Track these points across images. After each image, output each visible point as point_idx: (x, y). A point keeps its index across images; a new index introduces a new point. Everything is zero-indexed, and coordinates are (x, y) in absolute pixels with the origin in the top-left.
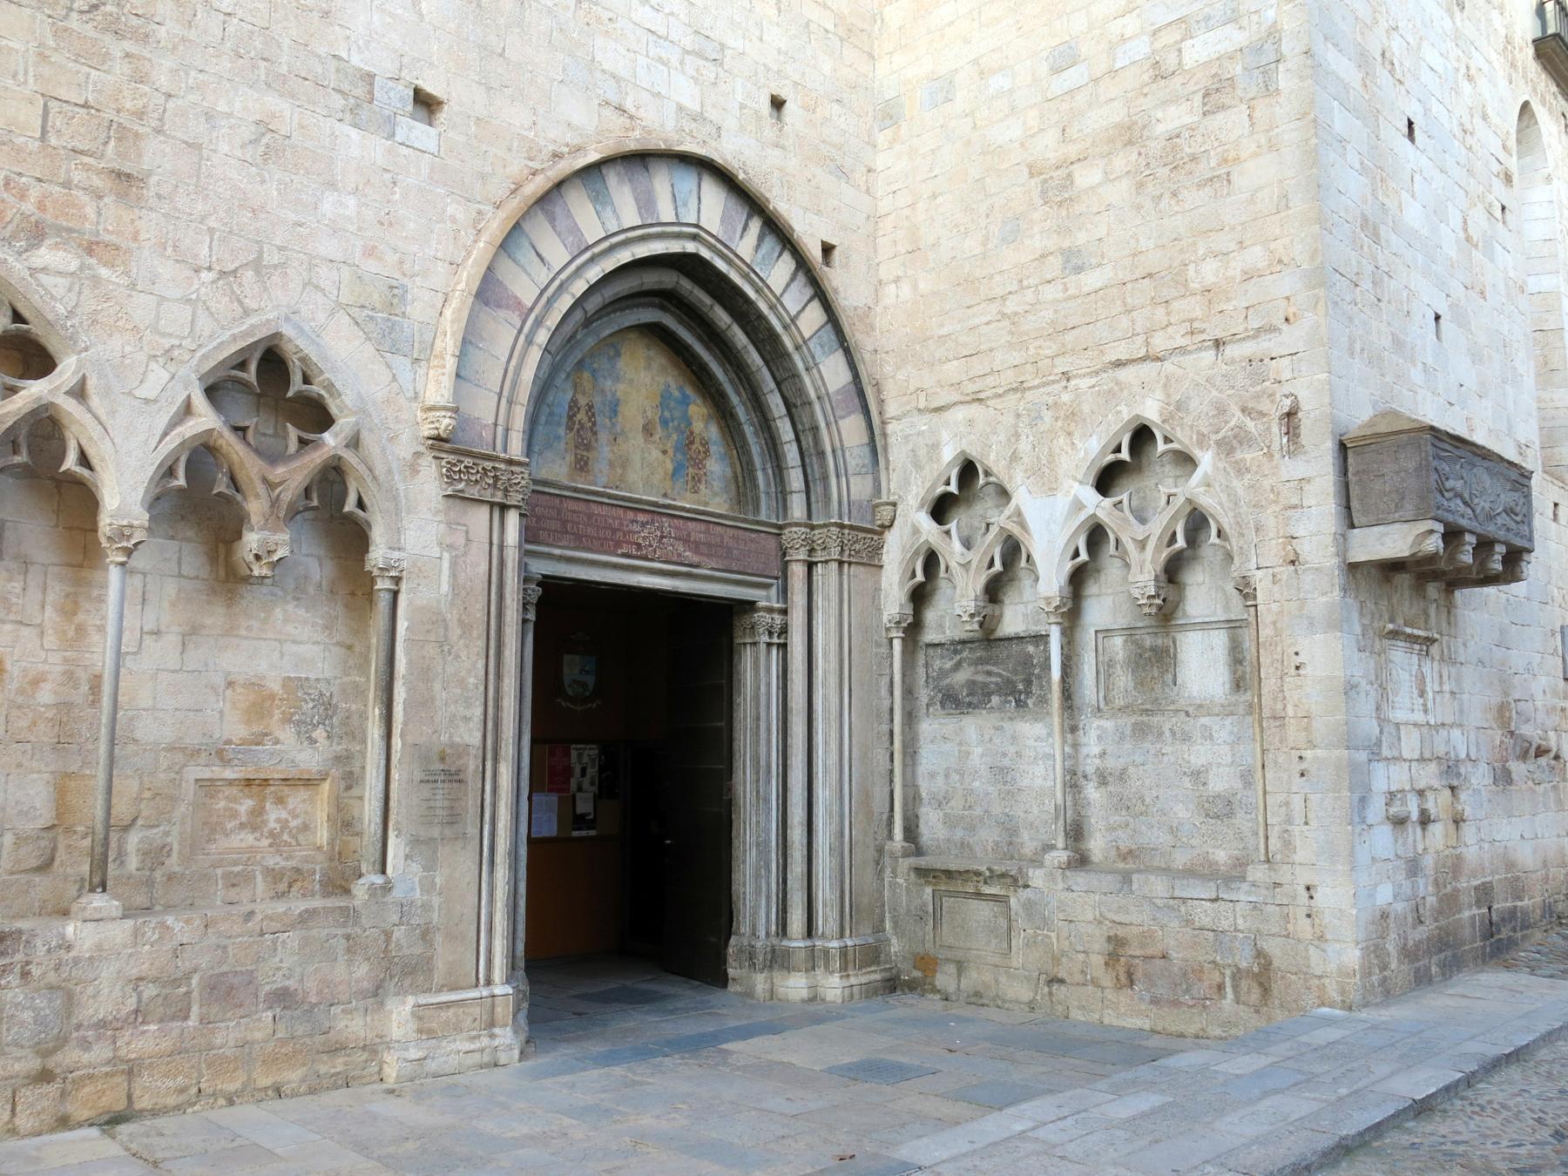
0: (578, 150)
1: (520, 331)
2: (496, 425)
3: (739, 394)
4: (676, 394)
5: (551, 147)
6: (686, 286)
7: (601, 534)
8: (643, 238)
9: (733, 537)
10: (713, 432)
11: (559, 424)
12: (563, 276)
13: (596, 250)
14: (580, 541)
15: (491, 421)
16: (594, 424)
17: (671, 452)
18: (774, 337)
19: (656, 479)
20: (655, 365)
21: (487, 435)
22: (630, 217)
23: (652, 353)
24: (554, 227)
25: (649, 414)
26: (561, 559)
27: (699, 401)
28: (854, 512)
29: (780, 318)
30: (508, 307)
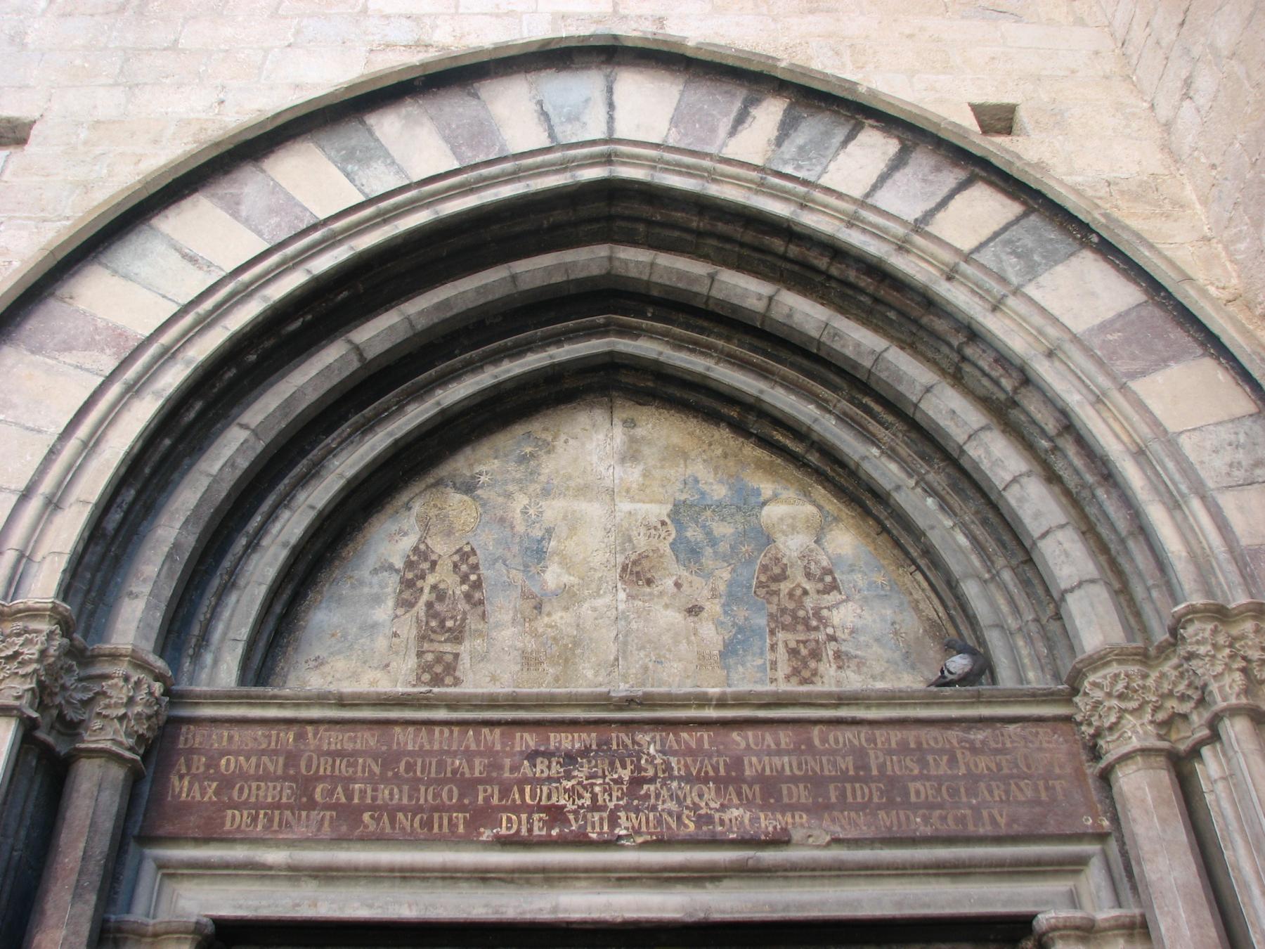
3: (872, 440)
4: (719, 492)
6: (634, 260)
7: (426, 796)
9: (904, 748)
10: (845, 541)
11: (377, 600)
14: (349, 822)
16: (477, 585)
17: (713, 608)
18: (877, 270)
20: (650, 454)
23: (639, 432)
24: (235, 215)
26: (295, 873)
27: (791, 493)
29: (879, 234)
30: (88, 346)
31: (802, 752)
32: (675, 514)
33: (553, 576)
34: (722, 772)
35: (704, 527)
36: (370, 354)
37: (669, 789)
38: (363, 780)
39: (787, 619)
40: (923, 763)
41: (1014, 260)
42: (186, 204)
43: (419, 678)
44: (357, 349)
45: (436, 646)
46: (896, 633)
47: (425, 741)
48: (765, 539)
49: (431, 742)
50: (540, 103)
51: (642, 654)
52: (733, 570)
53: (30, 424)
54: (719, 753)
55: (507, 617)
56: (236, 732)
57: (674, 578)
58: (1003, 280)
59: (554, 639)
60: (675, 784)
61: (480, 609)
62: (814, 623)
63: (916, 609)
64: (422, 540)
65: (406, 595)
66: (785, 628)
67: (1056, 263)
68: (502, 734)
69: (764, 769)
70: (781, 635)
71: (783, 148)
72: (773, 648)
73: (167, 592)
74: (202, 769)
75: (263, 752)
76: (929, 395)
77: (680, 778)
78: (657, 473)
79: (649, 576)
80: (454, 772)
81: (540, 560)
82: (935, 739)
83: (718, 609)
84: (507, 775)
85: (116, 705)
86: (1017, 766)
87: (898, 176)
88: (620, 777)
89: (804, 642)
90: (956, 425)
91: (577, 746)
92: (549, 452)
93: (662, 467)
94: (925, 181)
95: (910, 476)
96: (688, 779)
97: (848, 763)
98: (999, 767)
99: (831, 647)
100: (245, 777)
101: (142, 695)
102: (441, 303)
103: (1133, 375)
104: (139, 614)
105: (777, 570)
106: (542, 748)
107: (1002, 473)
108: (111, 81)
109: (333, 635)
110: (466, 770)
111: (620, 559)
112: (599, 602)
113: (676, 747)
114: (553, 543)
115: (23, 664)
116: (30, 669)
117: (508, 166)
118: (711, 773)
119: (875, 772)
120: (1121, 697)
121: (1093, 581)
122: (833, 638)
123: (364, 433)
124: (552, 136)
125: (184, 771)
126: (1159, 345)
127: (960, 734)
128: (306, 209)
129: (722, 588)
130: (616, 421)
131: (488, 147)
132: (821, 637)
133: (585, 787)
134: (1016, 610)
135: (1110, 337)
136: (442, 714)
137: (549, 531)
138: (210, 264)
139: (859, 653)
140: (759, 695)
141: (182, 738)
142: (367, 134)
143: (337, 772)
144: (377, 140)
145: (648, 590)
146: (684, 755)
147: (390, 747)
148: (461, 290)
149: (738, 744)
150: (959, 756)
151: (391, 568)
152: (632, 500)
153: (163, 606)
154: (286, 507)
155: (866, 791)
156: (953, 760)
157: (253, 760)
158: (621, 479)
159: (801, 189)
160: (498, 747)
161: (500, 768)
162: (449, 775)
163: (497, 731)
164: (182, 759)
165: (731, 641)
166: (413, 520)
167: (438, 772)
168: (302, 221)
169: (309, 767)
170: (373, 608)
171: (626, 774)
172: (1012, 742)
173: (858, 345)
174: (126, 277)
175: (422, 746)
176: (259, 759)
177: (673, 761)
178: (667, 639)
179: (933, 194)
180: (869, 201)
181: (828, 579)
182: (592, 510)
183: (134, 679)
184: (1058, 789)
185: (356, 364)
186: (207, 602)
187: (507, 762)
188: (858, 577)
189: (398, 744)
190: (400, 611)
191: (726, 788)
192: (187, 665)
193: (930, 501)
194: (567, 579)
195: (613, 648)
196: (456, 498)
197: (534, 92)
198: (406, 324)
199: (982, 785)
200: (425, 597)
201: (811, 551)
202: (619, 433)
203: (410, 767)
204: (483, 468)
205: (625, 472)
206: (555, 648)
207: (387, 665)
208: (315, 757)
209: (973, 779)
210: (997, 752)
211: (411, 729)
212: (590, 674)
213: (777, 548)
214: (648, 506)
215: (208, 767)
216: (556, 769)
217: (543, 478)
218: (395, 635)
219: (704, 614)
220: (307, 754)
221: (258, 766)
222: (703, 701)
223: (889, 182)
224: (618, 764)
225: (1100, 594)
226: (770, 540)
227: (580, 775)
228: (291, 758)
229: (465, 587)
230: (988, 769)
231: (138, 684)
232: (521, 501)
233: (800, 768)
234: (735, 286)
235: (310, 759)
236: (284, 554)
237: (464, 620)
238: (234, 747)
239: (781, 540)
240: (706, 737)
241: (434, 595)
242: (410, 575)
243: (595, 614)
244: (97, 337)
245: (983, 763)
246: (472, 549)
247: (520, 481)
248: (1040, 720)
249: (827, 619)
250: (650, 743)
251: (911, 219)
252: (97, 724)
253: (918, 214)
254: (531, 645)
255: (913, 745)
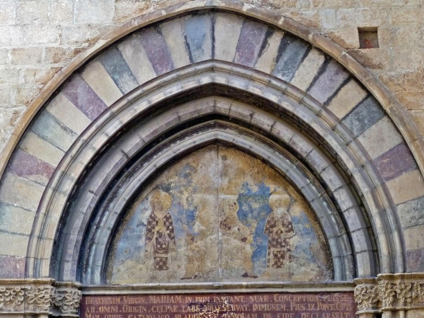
0: (91, 42)
1: (47, 187)
2: (27, 257)
4: (255, 189)
5: (73, 48)
6: (223, 105)
8: (160, 87)
9: (302, 302)
10: (297, 210)
11: (139, 237)
12: (85, 137)
13: (115, 109)
15: (23, 256)
16: (172, 231)
17: (250, 238)
19: (237, 263)
21: (20, 267)
22: (146, 73)
23: (228, 162)
24: (76, 105)
25: (227, 211)
27: (280, 190)
28: (410, 262)
29: (310, 109)
30: (38, 172)
31: (271, 303)
32: (239, 199)
33: (197, 227)
34: (246, 310)
35: (249, 205)
36: (131, 155)
37: (230, 315)
38: (142, 314)
39: (275, 243)
40: (307, 306)
41: (357, 123)
42: (57, 98)
43: (155, 267)
44: (126, 155)
45: (160, 255)
46: (311, 248)
47: (159, 300)
48: (269, 209)
49: (160, 301)
50: (186, 37)
51: (226, 257)
52: (258, 223)
53: (26, 208)
54: (246, 303)
55: (183, 242)
56: (102, 298)
57: (238, 226)
58: (351, 133)
59: (198, 251)
60: (232, 314)
61: (173, 240)
62: (283, 244)
63: (319, 238)
64: (153, 212)
65: (149, 235)
66: (274, 246)
67: (373, 123)
68: (182, 297)
69: (258, 309)
70: (272, 249)
71: (279, 63)
72: (269, 254)
73: (77, 258)
74: (94, 311)
75: (111, 305)
76: (324, 172)
77: (234, 312)
78: (234, 181)
79: (229, 226)
80: (168, 310)
81: (193, 220)
82: (312, 298)
83: (252, 239)
84: (183, 311)
85: (70, 301)
86: (335, 308)
87: (321, 78)
88: (216, 312)
89: (279, 252)
90: (332, 184)
91: (204, 301)
92: (195, 172)
93: (235, 179)
94: (331, 80)
95: (319, 192)
96: (236, 312)
97: (284, 307)
98: (330, 308)
99: (287, 255)
100: (107, 313)
101: (76, 297)
102: (154, 131)
103: (388, 179)
104: (70, 268)
105: (273, 223)
106: (193, 302)
107: (344, 206)
108: (14, 23)
109: (126, 251)
110: (172, 310)
111: (220, 219)
112: (213, 237)
113: (233, 301)
114: (197, 213)
115: (46, 299)
116: (48, 301)
117: (174, 75)
118: (243, 310)
119: (292, 310)
120: (363, 295)
121: (365, 251)
122: (289, 250)
123: (130, 177)
124: (191, 58)
125: (89, 312)
126: (401, 164)
127: (320, 297)
128: (102, 101)
129: (254, 230)
130: (219, 157)
131: (167, 65)
132: (285, 249)
133: (206, 315)
134: (346, 249)
135: (384, 161)
136: (163, 292)
137: (196, 208)
138: (72, 132)
139: (297, 256)
140: (258, 285)
141: (86, 301)
142: (120, 57)
143: (134, 311)
144: (124, 60)
145: (229, 232)
146: (235, 304)
147: (148, 302)
148: (161, 125)
149: (252, 300)
150: (318, 304)
151: (143, 224)
152: (225, 194)
153: (76, 263)
154: (107, 210)
155: (288, 316)
156: (316, 306)
157: (109, 308)
158: (221, 184)
159: (284, 86)
160: (180, 302)
161: (181, 309)
162: (167, 311)
163: (180, 297)
164: (88, 308)
165: (255, 251)
166: (149, 204)
167: (163, 311)
168: (101, 108)
169: (125, 310)
170: (138, 240)
171: (218, 310)
172: (336, 299)
173: (301, 149)
174: (43, 138)
175: (158, 302)
176: (110, 307)
177: (232, 306)
178: (234, 251)
179: (333, 88)
180: (308, 93)
181: (290, 226)
182: (211, 198)
183: (73, 293)
184: (347, 316)
185: (125, 160)
186: (87, 252)
187: (183, 307)
188: (300, 225)
189: (151, 301)
190: (147, 242)
191: (247, 315)
192: (84, 275)
193: (325, 203)
194: (203, 228)
195: (217, 254)
196: (163, 194)
197: (183, 31)
198: (142, 141)
199: (324, 314)
200: (155, 236)
201: (285, 215)
202: (220, 161)
203: (155, 309)
204: (172, 180)
205: (222, 181)
206: (198, 255)
207: (145, 263)
208: (127, 306)
209: (321, 312)
210: (330, 303)
211: (154, 296)
212: (209, 265)
213: (273, 213)
214: (230, 196)
215: (96, 310)
216: (198, 309)
217: (193, 184)
218: (146, 251)
219: (247, 241)
220: (124, 305)
221: (110, 310)
222: (241, 287)
223: (318, 81)
224: (216, 307)
225: (367, 255)
226: (271, 210)
227: (205, 311)
228: (120, 307)
229: (168, 232)
230: (326, 309)
231: (75, 293)
232: (186, 195)
233: (269, 308)
234: (260, 120)
235: (125, 307)
236: (109, 232)
237: (168, 244)
238: (102, 304)
239: (275, 210)
240: (242, 298)
241: (158, 235)
242: (149, 227)
243: (211, 242)
244: (39, 168)
245: (325, 306)
246: (170, 216)
247: (184, 186)
248: (345, 292)
249: (288, 243)
250: (225, 300)
251: (322, 102)
252: (65, 308)
253: (325, 100)
254: (191, 254)
255: (304, 300)
